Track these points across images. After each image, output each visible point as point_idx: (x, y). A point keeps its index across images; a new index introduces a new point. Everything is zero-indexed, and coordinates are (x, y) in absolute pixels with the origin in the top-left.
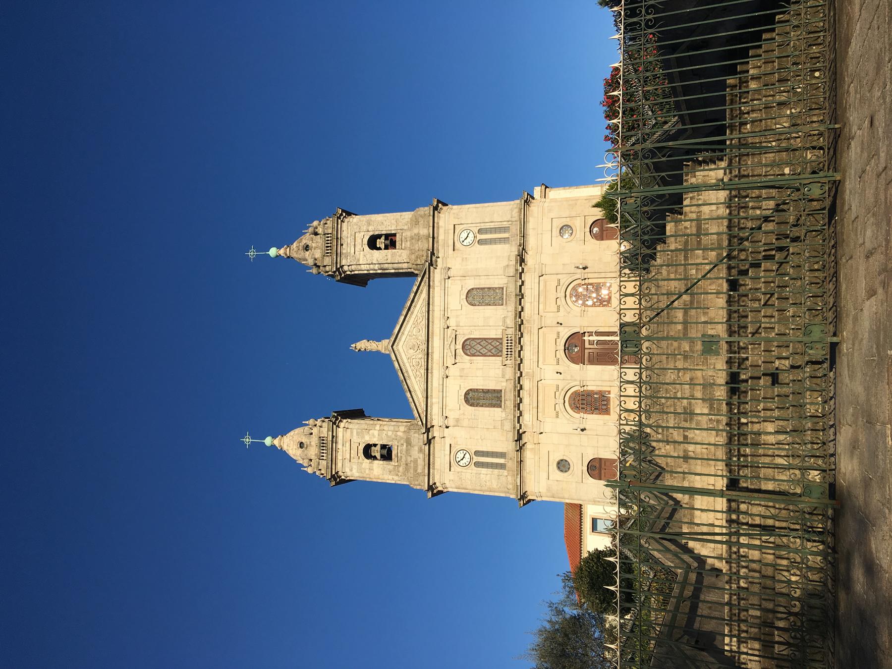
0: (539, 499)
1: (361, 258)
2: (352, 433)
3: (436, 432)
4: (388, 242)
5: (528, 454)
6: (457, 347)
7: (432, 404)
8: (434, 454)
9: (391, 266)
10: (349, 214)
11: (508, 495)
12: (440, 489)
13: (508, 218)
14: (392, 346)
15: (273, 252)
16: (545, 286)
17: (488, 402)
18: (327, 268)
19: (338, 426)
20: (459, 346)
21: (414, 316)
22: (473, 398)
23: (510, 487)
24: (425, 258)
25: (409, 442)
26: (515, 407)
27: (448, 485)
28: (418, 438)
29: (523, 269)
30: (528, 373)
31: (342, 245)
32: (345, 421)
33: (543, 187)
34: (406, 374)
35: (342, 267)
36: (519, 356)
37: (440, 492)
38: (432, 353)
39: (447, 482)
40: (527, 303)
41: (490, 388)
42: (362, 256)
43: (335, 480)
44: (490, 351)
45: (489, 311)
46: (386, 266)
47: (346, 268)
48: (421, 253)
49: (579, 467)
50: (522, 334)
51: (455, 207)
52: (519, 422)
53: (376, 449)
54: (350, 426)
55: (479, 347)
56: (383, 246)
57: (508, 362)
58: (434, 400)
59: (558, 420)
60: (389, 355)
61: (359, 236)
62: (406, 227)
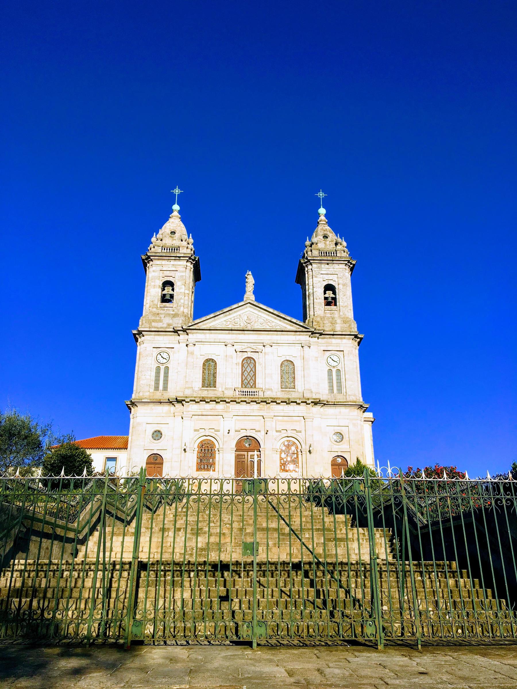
0: (131, 416)
1: (317, 278)
2: (183, 272)
3: (183, 336)
4: (330, 300)
5: (166, 408)
6: (249, 353)
7: (205, 333)
8: (166, 335)
9: (312, 302)
10: (352, 270)
11: (134, 392)
12: (139, 340)
13: (349, 393)
14: (249, 303)
15: (322, 211)
16: (296, 421)
17: (206, 377)
18: (309, 253)
19: (188, 261)
20: (249, 355)
21: (273, 320)
22: (210, 367)
23: (141, 394)
24: (318, 328)
25: (175, 316)
26: (203, 398)
27: (142, 346)
29: (309, 404)
30: (229, 407)
31: (328, 264)
32: (192, 266)
33: (372, 420)
34: (228, 313)
35: (311, 264)
36: (242, 401)
37: (137, 340)
38: (245, 334)
39: (145, 345)
40: (283, 407)
42: (319, 279)
43: (146, 259)
44: (246, 378)
45: (277, 378)
46: (311, 298)
47: (310, 267)
48: (321, 325)
49: (156, 447)
50: (259, 403)
51: (357, 352)
52: (191, 401)
53: (170, 290)
54: (188, 271)
55: (249, 370)
56: (327, 296)
57: (237, 393)
58: (208, 335)
60: (242, 300)
61: (334, 277)
62: (341, 313)
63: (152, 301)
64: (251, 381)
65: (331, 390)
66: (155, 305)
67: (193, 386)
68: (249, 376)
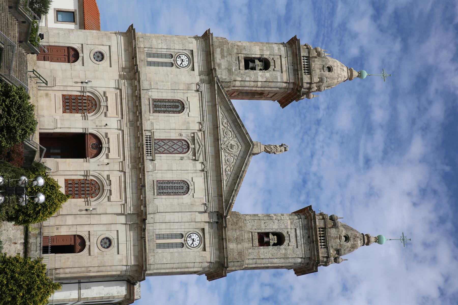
2: (282, 78)
6: (193, 146)
20: (192, 146)
23: (141, 39)
25: (230, 71)
28: (222, 74)
41: (163, 114)
42: (289, 227)
45: (169, 177)
48: (234, 227)
49: (86, 55)
56: (271, 236)
57: (149, 134)
59: (104, 89)
63: (244, 48)
64: (163, 150)
65: (159, 236)
66: (241, 51)
67: (153, 90)
68: (168, 147)
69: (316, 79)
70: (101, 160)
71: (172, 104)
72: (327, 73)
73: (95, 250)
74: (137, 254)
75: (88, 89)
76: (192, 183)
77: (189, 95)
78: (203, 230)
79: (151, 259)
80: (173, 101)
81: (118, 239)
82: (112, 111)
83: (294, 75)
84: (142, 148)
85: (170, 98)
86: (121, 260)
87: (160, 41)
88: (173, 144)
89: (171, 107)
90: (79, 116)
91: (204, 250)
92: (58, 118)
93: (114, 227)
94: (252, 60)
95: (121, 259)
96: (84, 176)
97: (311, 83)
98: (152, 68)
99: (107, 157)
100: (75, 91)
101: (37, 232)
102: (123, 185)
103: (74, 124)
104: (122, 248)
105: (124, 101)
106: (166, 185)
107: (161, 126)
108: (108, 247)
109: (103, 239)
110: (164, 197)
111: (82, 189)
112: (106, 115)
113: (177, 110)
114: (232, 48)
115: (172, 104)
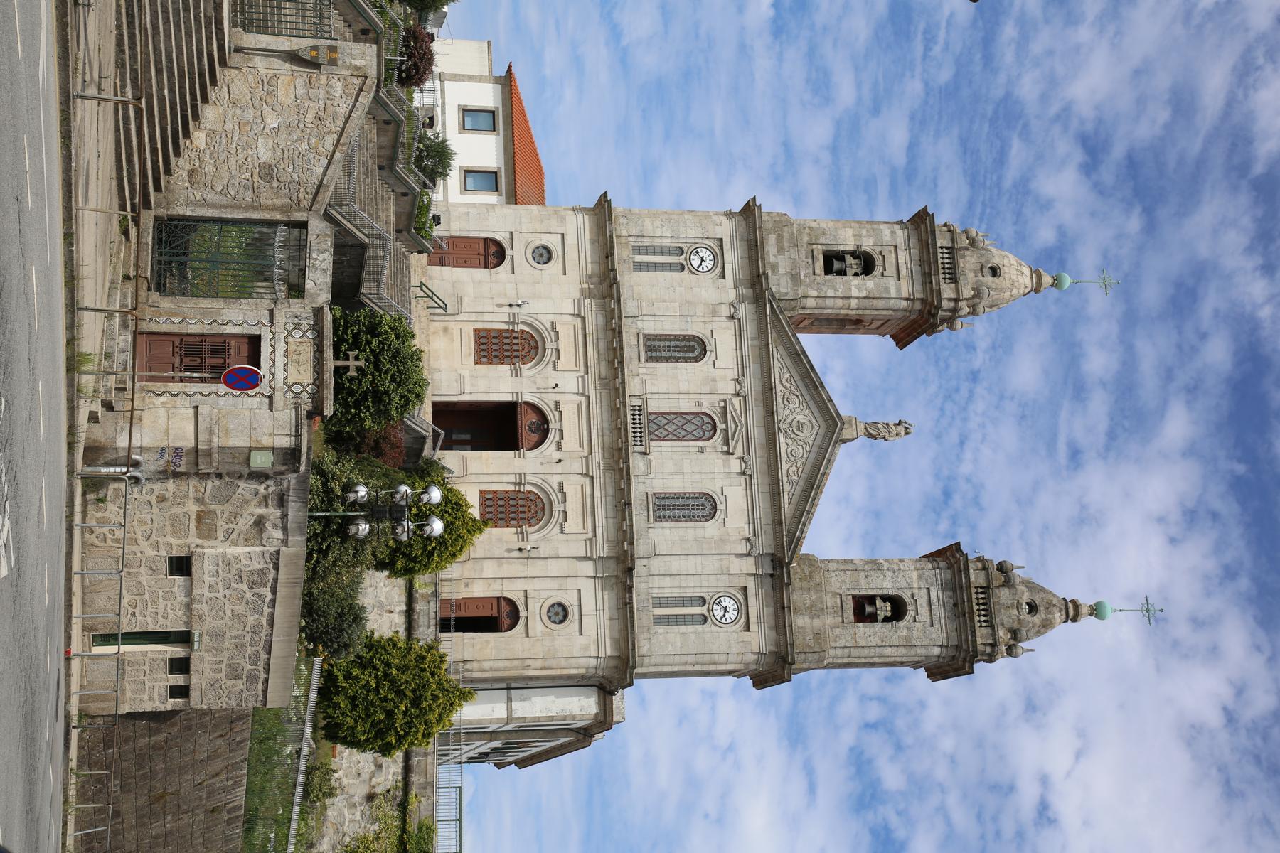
2: (899, 291)
6: (724, 426)
20: (721, 426)
23: (622, 220)
25: (795, 278)
28: (779, 284)
41: (664, 364)
42: (916, 585)
48: (805, 584)
49: (518, 252)
55: (689, 427)
56: (879, 603)
57: (637, 402)
59: (552, 318)
62: (837, 631)
65: (660, 602)
69: (967, 292)
70: (547, 453)
71: (682, 344)
72: (989, 279)
73: (537, 627)
74: (616, 635)
75: (523, 318)
76: (723, 498)
77: (714, 326)
78: (745, 589)
79: (643, 646)
80: (685, 338)
81: (580, 605)
82: (566, 360)
83: (924, 283)
84: (625, 431)
85: (678, 332)
86: (586, 648)
87: (658, 223)
88: (683, 421)
89: (680, 349)
90: (504, 369)
91: (748, 628)
92: (466, 373)
93: (571, 583)
94: (840, 256)
95: (586, 644)
96: (515, 484)
97: (956, 300)
98: (643, 274)
99: (559, 448)
100: (497, 321)
101: (429, 590)
102: (588, 501)
103: (495, 384)
104: (589, 622)
105: (589, 339)
106: (671, 501)
107: (661, 386)
108: (561, 622)
109: (553, 606)
110: (667, 525)
111: (512, 509)
112: (555, 367)
113: (692, 355)
114: (800, 233)
115: (682, 344)
